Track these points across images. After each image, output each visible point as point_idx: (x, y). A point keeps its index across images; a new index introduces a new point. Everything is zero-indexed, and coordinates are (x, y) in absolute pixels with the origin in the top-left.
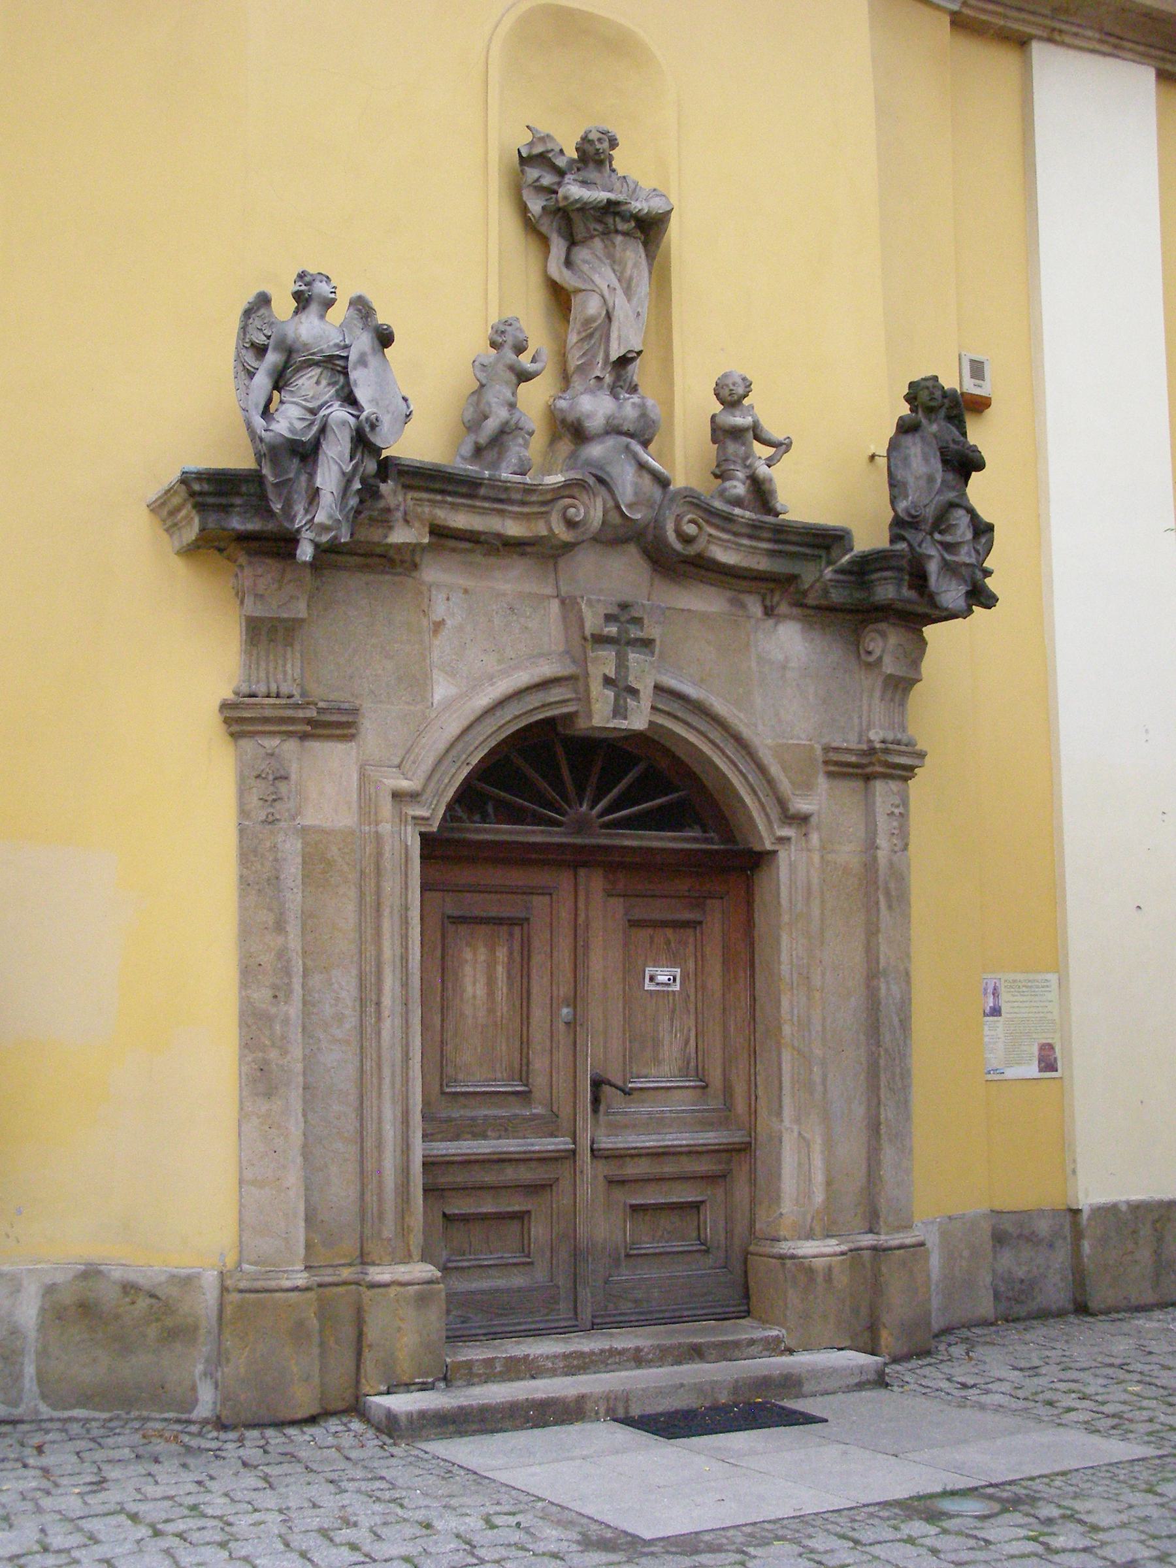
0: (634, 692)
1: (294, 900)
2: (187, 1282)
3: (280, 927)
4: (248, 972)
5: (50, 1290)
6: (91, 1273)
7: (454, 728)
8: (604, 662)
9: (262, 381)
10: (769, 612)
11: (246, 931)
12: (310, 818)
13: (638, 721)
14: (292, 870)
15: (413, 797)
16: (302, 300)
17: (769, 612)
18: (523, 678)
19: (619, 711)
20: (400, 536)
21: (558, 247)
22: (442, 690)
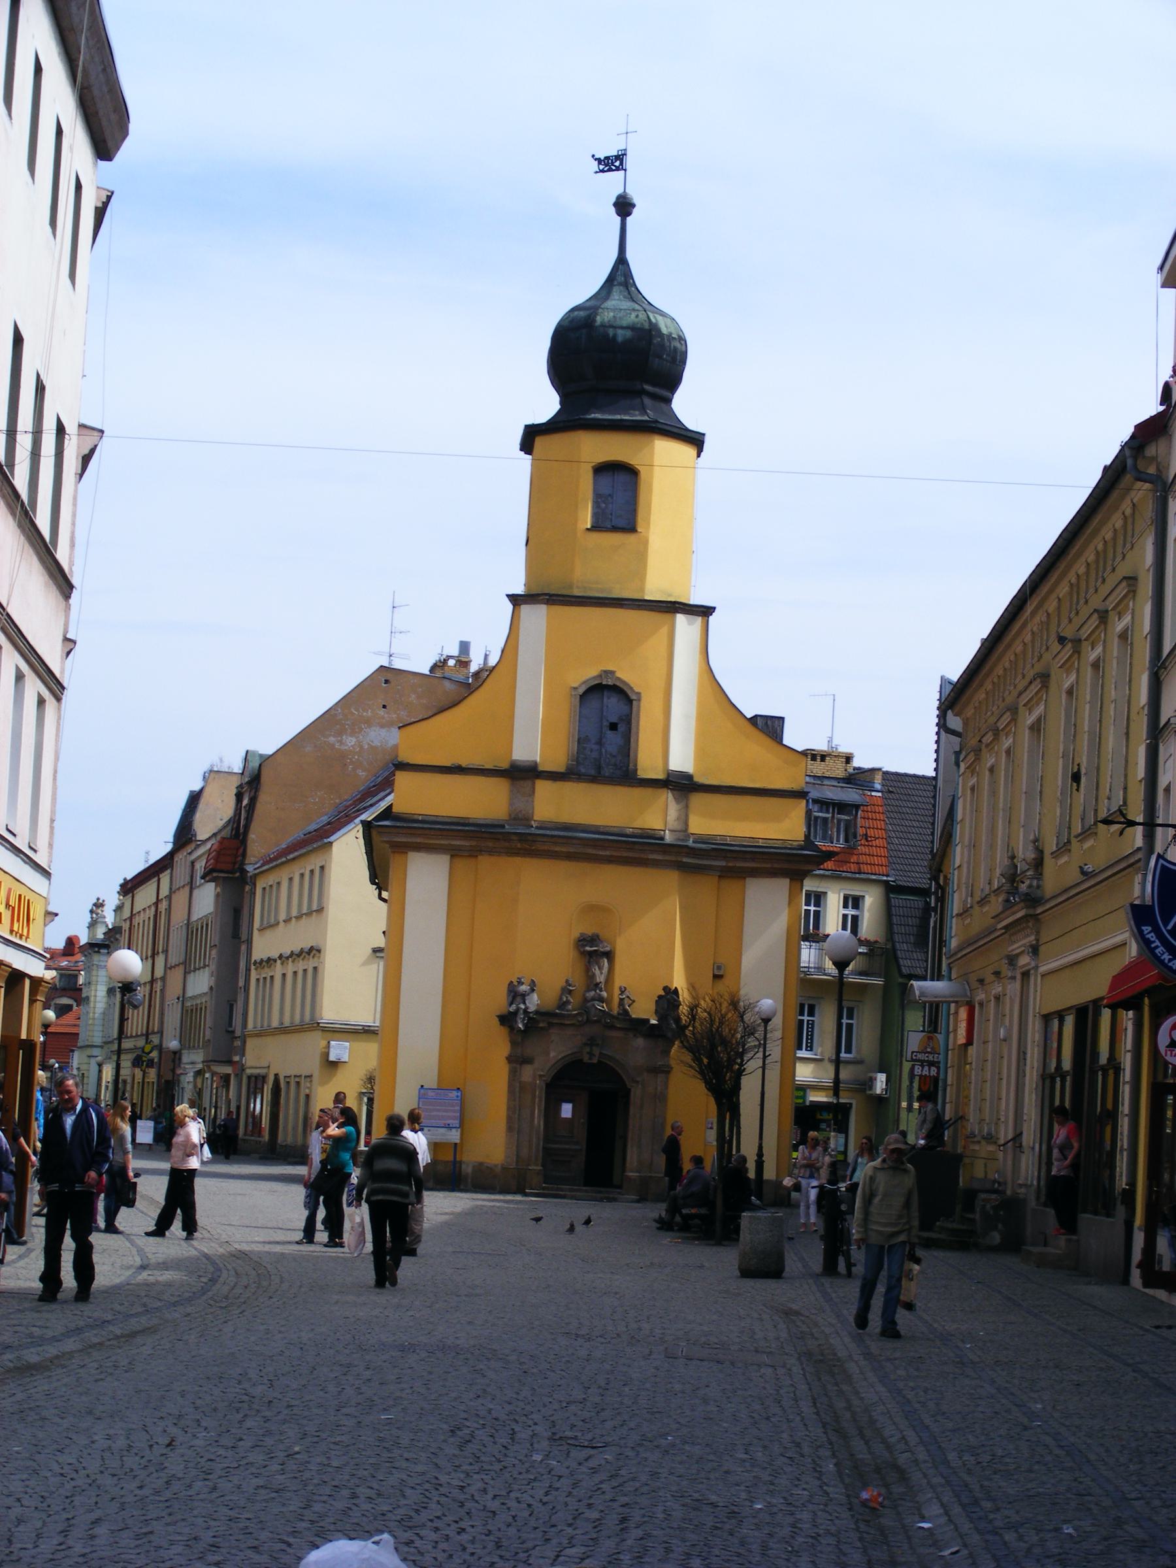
0: (594, 1055)
1: (518, 1095)
2: (496, 1166)
3: (514, 1100)
4: (509, 1108)
5: (474, 1166)
6: (481, 1164)
7: (554, 1061)
8: (588, 1049)
9: (510, 998)
10: (635, 1036)
11: (509, 1100)
12: (523, 1079)
13: (595, 1061)
14: (517, 1089)
15: (543, 1076)
16: (519, 982)
17: (635, 1036)
18: (569, 1052)
19: (590, 1059)
20: (541, 1025)
21: (588, 957)
22: (552, 1054)
